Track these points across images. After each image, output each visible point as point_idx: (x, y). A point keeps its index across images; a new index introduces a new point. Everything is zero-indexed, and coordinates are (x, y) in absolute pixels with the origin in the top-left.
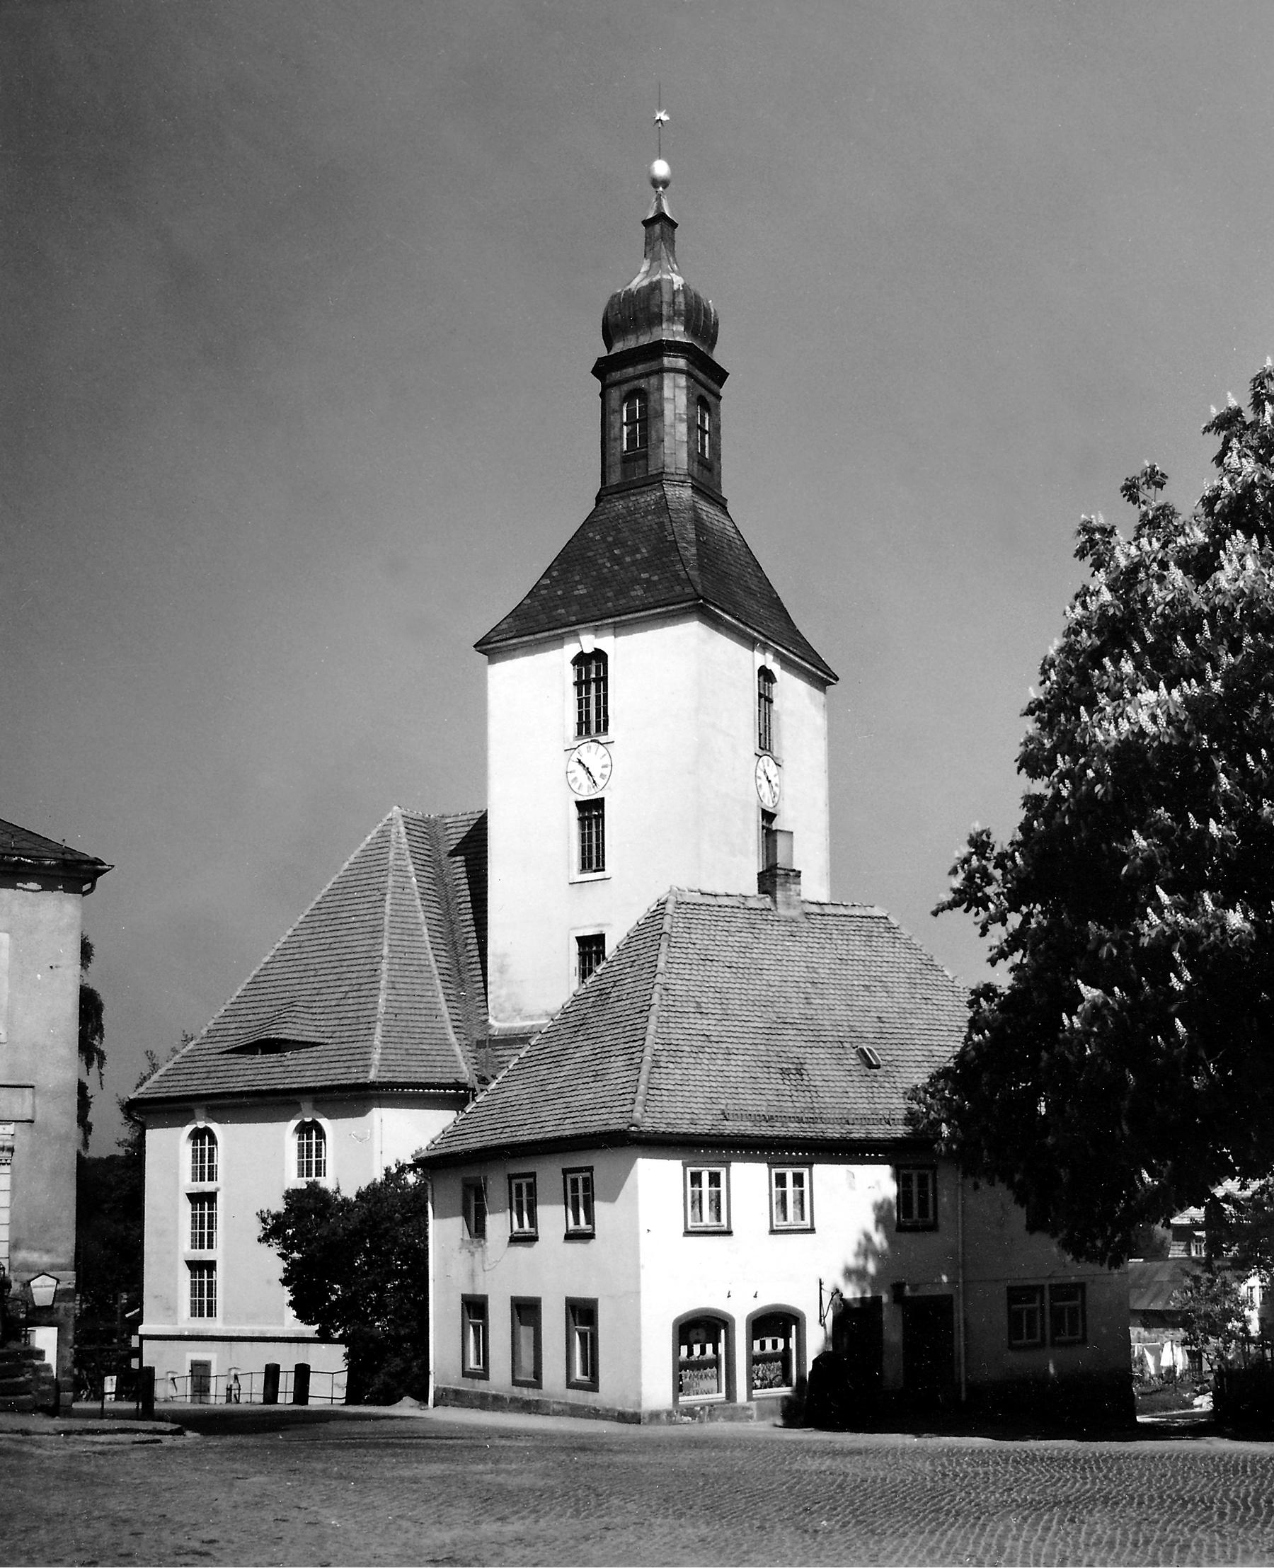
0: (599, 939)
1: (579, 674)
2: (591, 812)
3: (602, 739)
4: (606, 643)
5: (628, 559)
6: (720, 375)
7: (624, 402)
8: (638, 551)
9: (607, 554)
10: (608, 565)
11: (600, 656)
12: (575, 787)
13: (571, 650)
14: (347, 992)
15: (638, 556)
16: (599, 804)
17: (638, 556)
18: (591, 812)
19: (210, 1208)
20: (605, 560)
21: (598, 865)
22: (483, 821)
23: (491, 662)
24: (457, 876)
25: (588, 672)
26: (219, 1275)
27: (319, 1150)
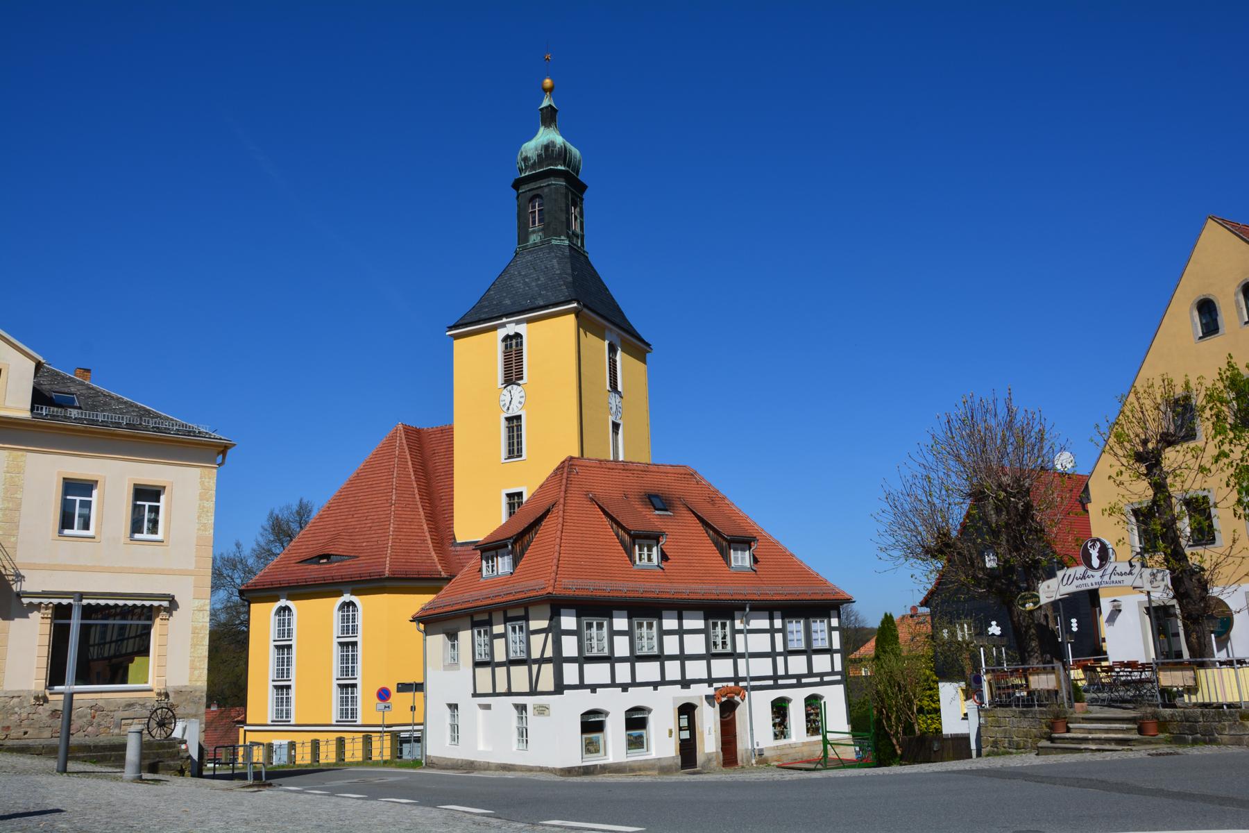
0: (520, 494)
1: (506, 347)
2: (514, 423)
3: (520, 382)
4: (522, 329)
5: (534, 284)
6: (582, 188)
7: (530, 202)
8: (539, 279)
11: (518, 336)
13: (502, 333)
14: (371, 527)
15: (539, 282)
16: (519, 418)
17: (539, 282)
18: (514, 423)
19: (288, 654)
21: (518, 452)
23: (455, 339)
25: (511, 344)
26: (293, 693)
27: (354, 619)
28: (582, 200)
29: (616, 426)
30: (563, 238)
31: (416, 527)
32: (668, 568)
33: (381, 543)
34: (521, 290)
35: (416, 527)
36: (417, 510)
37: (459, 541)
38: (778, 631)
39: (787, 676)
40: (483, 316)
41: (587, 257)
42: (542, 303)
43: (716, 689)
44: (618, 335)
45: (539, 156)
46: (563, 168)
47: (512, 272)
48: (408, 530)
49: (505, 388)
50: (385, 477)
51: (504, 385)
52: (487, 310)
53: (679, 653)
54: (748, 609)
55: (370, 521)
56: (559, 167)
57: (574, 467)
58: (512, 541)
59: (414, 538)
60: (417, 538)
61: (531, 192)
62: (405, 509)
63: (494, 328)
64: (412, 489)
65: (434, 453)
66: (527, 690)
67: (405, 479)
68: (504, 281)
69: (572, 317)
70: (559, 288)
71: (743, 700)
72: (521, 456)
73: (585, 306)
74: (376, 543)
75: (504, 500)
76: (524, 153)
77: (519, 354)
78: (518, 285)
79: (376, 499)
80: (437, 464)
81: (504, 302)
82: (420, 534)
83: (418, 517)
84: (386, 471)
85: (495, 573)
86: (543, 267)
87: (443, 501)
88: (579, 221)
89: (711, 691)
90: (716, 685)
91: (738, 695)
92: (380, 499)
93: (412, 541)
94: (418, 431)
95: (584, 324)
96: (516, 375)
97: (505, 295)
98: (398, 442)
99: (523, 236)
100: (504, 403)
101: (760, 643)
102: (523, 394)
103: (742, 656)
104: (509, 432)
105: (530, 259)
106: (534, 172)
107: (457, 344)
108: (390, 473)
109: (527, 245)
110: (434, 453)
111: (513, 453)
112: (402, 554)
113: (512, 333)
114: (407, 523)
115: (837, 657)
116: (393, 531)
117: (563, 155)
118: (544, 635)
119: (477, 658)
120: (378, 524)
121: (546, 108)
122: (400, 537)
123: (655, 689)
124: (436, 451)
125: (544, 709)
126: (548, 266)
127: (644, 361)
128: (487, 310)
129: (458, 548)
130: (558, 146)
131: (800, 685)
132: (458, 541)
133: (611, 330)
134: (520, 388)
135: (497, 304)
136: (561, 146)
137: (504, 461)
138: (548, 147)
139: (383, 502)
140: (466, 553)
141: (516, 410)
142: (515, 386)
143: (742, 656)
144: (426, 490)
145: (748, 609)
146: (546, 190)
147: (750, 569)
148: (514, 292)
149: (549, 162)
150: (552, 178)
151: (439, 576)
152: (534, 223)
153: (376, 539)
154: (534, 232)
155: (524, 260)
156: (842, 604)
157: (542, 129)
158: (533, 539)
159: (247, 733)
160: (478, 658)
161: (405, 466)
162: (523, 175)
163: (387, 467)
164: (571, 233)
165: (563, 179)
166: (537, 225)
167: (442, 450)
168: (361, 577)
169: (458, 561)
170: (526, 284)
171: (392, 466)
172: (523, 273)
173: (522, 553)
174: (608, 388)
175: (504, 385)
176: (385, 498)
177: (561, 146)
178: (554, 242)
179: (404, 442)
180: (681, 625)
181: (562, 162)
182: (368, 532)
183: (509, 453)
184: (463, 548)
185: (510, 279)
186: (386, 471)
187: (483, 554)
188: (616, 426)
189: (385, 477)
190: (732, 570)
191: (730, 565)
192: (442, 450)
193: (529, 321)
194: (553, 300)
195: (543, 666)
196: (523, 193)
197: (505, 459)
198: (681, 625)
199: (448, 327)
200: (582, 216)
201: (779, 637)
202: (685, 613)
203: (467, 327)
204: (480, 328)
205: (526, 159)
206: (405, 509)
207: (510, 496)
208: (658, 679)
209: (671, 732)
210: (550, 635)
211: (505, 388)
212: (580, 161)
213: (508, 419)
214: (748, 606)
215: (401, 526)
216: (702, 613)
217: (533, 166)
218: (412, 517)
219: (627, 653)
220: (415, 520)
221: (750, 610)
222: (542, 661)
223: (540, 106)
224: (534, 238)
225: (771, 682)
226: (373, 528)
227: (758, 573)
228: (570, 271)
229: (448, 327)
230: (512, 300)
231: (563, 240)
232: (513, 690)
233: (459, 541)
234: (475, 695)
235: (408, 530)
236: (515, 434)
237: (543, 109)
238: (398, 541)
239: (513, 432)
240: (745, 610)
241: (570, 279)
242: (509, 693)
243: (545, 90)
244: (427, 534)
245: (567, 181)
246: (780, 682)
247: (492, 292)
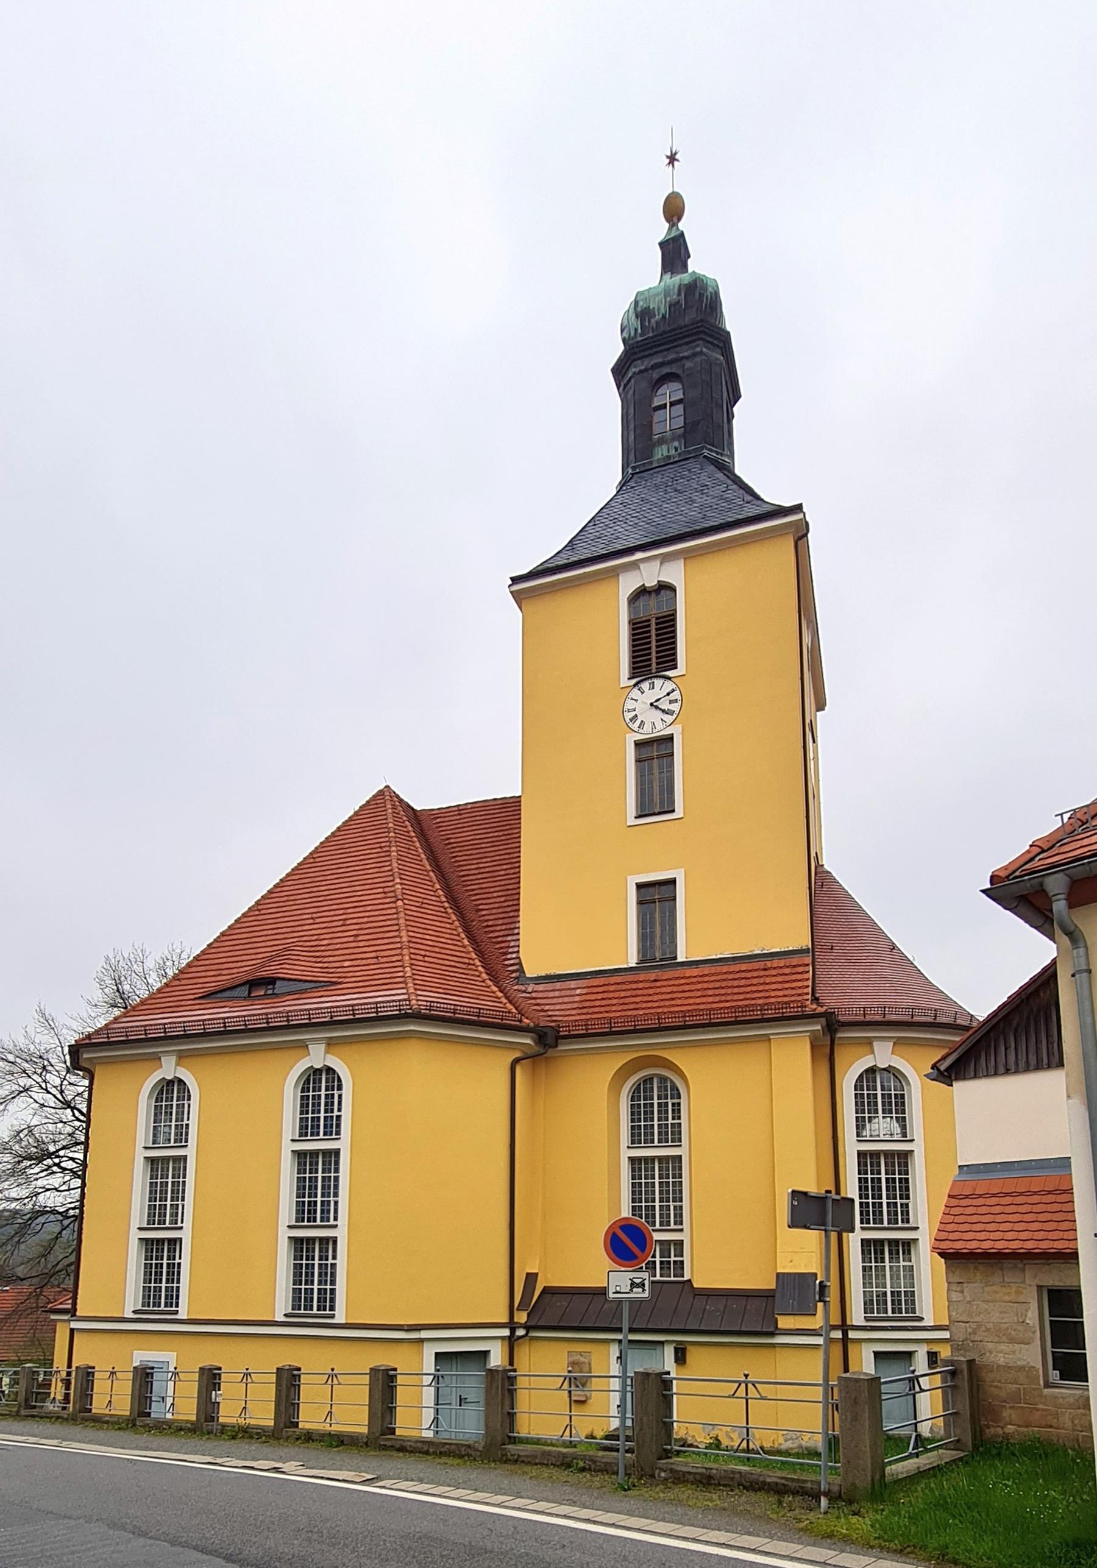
3: (669, 673)
4: (674, 574)
13: (628, 584)
45: (673, 306)
51: (634, 681)
100: (633, 714)
113: (651, 583)
137: (632, 821)
141: (659, 725)
159: (76, 1334)
175: (634, 681)
211: (635, 685)
213: (638, 744)
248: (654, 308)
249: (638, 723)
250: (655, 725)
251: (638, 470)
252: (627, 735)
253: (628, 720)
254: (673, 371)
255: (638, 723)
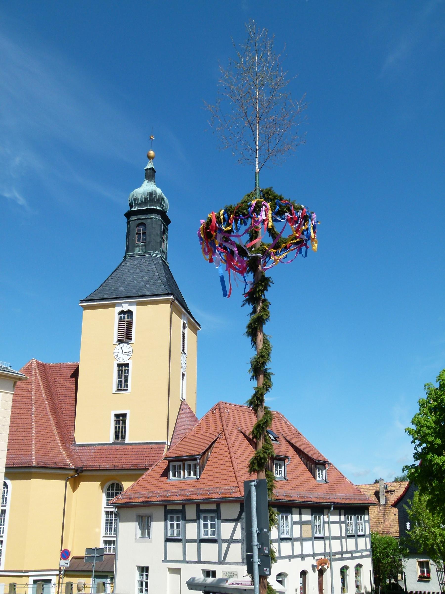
3: (130, 342)
4: (133, 308)
5: (140, 280)
8: (143, 277)
9: (131, 277)
10: (132, 281)
11: (130, 312)
12: (117, 358)
13: (118, 309)
14: (17, 429)
15: (144, 279)
16: (127, 365)
17: (144, 279)
20: (131, 279)
21: (124, 387)
22: (79, 365)
24: (57, 387)
25: (124, 318)
28: (167, 230)
29: (183, 375)
30: (157, 252)
31: (49, 431)
32: (291, 479)
33: (26, 441)
34: (131, 283)
35: (49, 431)
36: (49, 419)
37: (77, 443)
38: (343, 522)
39: (347, 552)
40: (105, 296)
41: (168, 266)
42: (148, 293)
43: (316, 560)
44: (188, 318)
45: (145, 199)
46: (160, 209)
47: (124, 270)
48: (44, 433)
49: (118, 344)
50: (25, 395)
51: (118, 343)
52: (107, 292)
53: (300, 537)
54: (332, 508)
55: (16, 425)
56: (158, 208)
57: (226, 409)
58: (200, 457)
59: (49, 439)
60: (51, 439)
61: (138, 221)
62: (41, 418)
63: (113, 306)
64: (44, 405)
65: (56, 381)
66: (217, 560)
67: (39, 397)
68: (118, 275)
69: (168, 306)
70: (158, 285)
71: (328, 567)
72: (127, 390)
73: (177, 299)
74: (22, 441)
75: (113, 418)
76: (135, 195)
77: (130, 324)
78: (129, 279)
79: (19, 410)
80: (58, 389)
81: (120, 289)
82: (52, 437)
83: (50, 424)
84: (26, 391)
85: (182, 477)
86: (146, 270)
87: (64, 414)
88: (165, 243)
89: (314, 563)
90: (317, 558)
91: (326, 564)
92: (22, 410)
93: (48, 441)
94: (43, 365)
95: (173, 308)
96: (126, 337)
97: (120, 284)
98: (33, 372)
99: (129, 248)
100: (117, 354)
101: (335, 530)
102: (131, 350)
103: (329, 538)
104: (119, 373)
105: (135, 263)
106: (141, 208)
107: (86, 313)
108: (29, 393)
109: (133, 254)
110: (56, 381)
111: (121, 387)
112: (43, 450)
113: (125, 310)
114: (43, 428)
115: (368, 539)
116: (35, 433)
117: (160, 201)
118: (233, 524)
119: (169, 535)
120: (22, 427)
121: (150, 169)
122: (39, 438)
123: (290, 560)
124: (57, 380)
125: (232, 575)
126: (150, 270)
127: (196, 334)
128: (107, 292)
129: (77, 448)
130: (158, 194)
131: (352, 558)
132: (77, 443)
133: (185, 314)
134: (129, 346)
135: (115, 290)
136: (160, 195)
138: (151, 194)
139: (25, 412)
140: (83, 451)
142: (125, 345)
143: (329, 538)
144: (52, 406)
145: (332, 508)
146: (149, 221)
147: (325, 482)
148: (126, 283)
149: (152, 204)
150: (153, 214)
151: (68, 467)
152: (139, 240)
153: (22, 438)
154: (138, 246)
155: (132, 263)
156: (370, 506)
157: (146, 182)
158: (209, 456)
160: (169, 536)
161: (39, 389)
162: (133, 209)
163: (27, 388)
164: (161, 250)
165: (160, 216)
166: (141, 242)
167: (62, 380)
168: (21, 464)
169: (78, 457)
170: (134, 278)
171: (30, 388)
172: (132, 272)
173: (204, 466)
174: (182, 351)
175: (118, 343)
176: (26, 410)
177: (160, 195)
178: (152, 254)
179: (37, 372)
180: (301, 518)
181: (159, 205)
182: (16, 433)
183: (118, 387)
184: (81, 448)
185: (123, 274)
186: (26, 391)
187: (170, 463)
188: (183, 375)
189: (25, 395)
190: (318, 482)
191: (316, 479)
192: (62, 380)
193: (139, 304)
194: (155, 292)
195: (232, 545)
196: (133, 220)
197: (115, 391)
198: (301, 518)
199: (80, 300)
200: (167, 240)
201: (343, 526)
202: (303, 510)
203: (94, 302)
204: (110, 303)
205: (136, 199)
206: (41, 418)
207: (117, 416)
208: (291, 554)
209: (296, 590)
210: (239, 524)
211: (118, 344)
212: (168, 205)
214: (333, 506)
215: (39, 430)
216: (310, 510)
217: (141, 204)
218: (46, 424)
219: (276, 537)
220: (48, 427)
221: (334, 509)
222: (231, 541)
223: (145, 167)
224: (137, 251)
225: (339, 556)
226: (18, 430)
227: (330, 484)
228: (164, 274)
229: (80, 300)
230: (126, 288)
231: (158, 254)
232: (203, 559)
233: (77, 443)
234: (166, 560)
235: (44, 433)
236: (123, 375)
237: (146, 170)
238: (37, 440)
239: (122, 373)
240: (330, 508)
241: (165, 280)
242: (199, 562)
243: (149, 158)
244: (57, 436)
245: (162, 217)
246: (344, 556)
247: (110, 281)
248: (139, 198)
249: (118, 357)
250: (123, 359)
251: (129, 256)
252: (115, 361)
253: (115, 356)
254: (144, 222)
255: (118, 357)
